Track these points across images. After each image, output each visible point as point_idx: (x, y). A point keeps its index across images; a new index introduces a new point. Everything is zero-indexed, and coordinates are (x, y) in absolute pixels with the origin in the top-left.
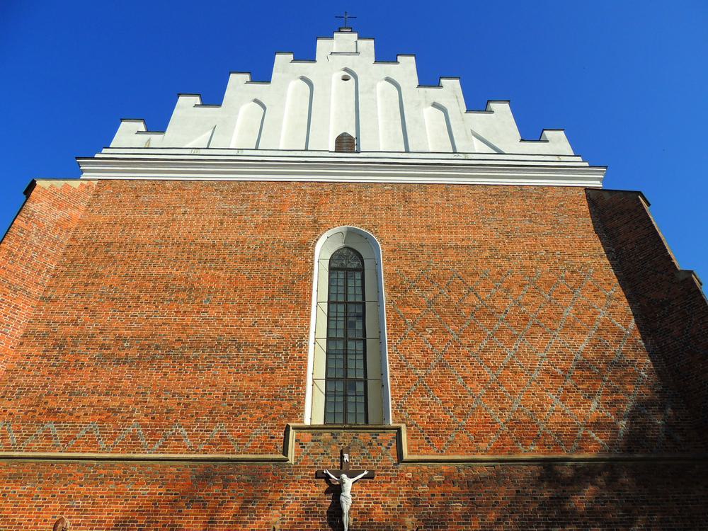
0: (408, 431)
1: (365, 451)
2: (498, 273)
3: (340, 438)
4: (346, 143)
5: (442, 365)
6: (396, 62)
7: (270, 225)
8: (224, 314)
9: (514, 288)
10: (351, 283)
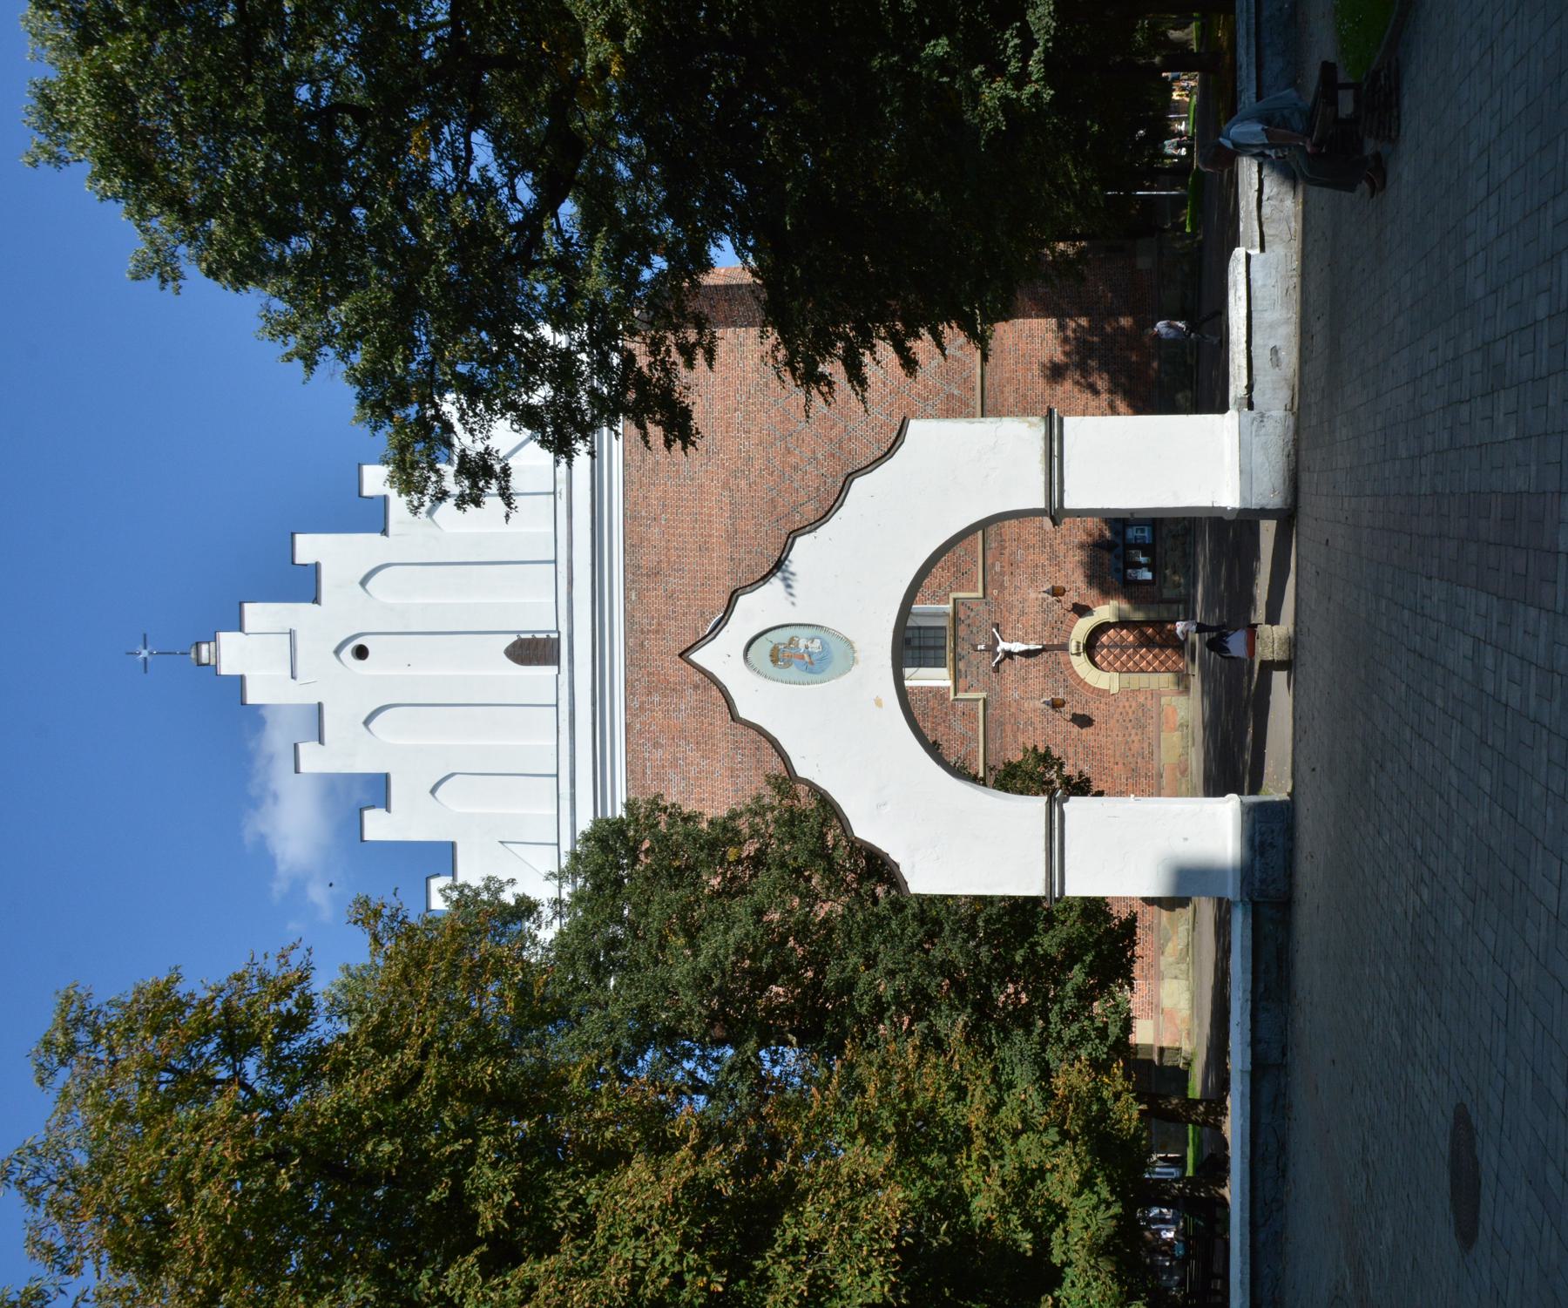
0: (957, 590)
2: (771, 474)
4: (532, 651)
6: (316, 567)
9: (792, 460)
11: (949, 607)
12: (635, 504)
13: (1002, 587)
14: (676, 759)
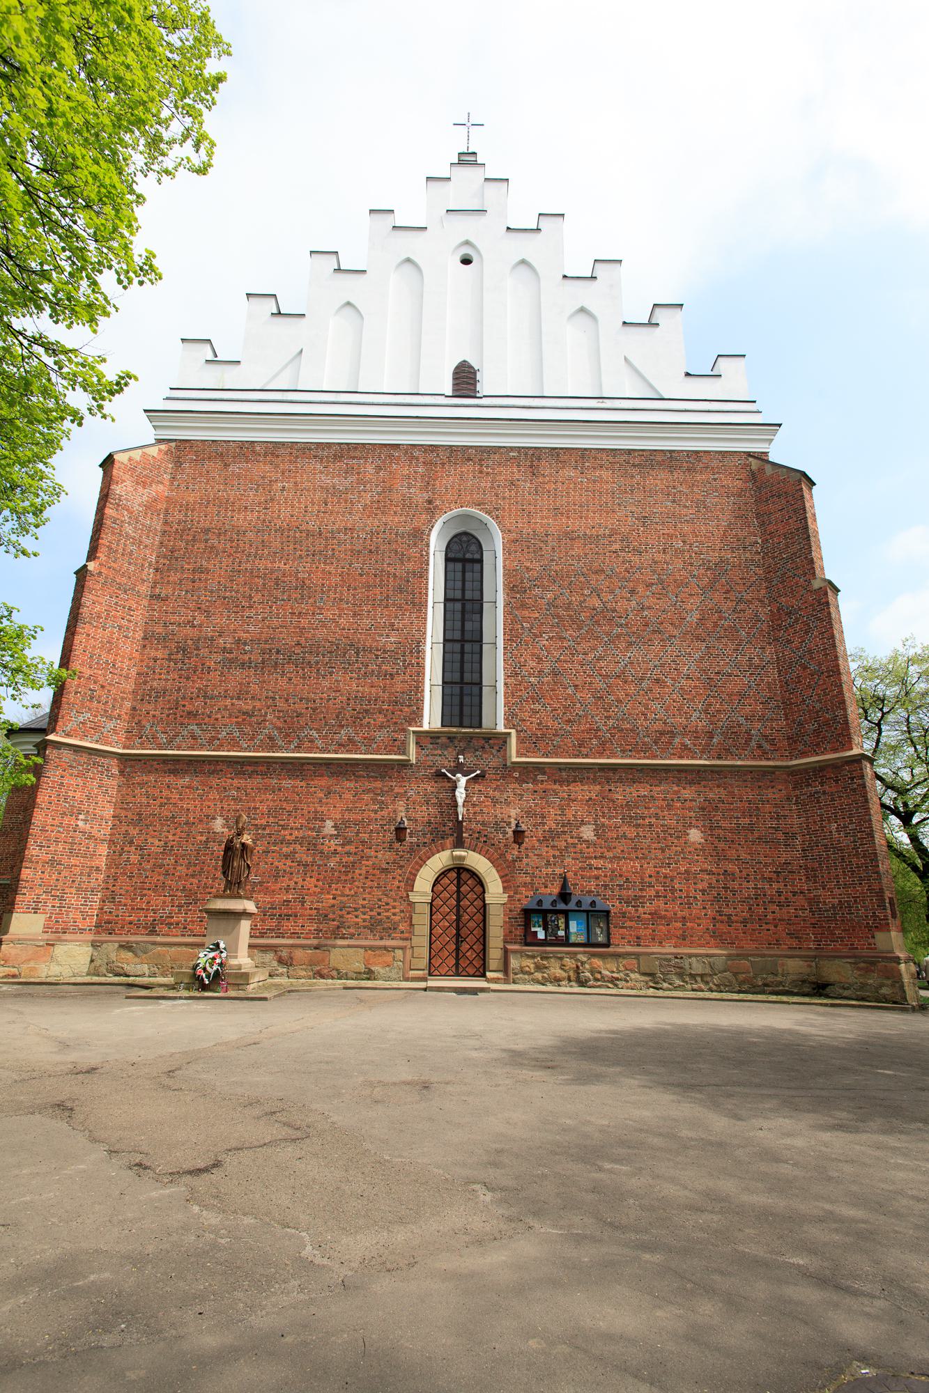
0: (518, 737)
3: (456, 742)
4: (465, 380)
5: (555, 673)
7: (379, 507)
8: (340, 616)
9: (640, 589)
10: (468, 575)
11: (501, 728)
12: (595, 458)
13: (521, 781)
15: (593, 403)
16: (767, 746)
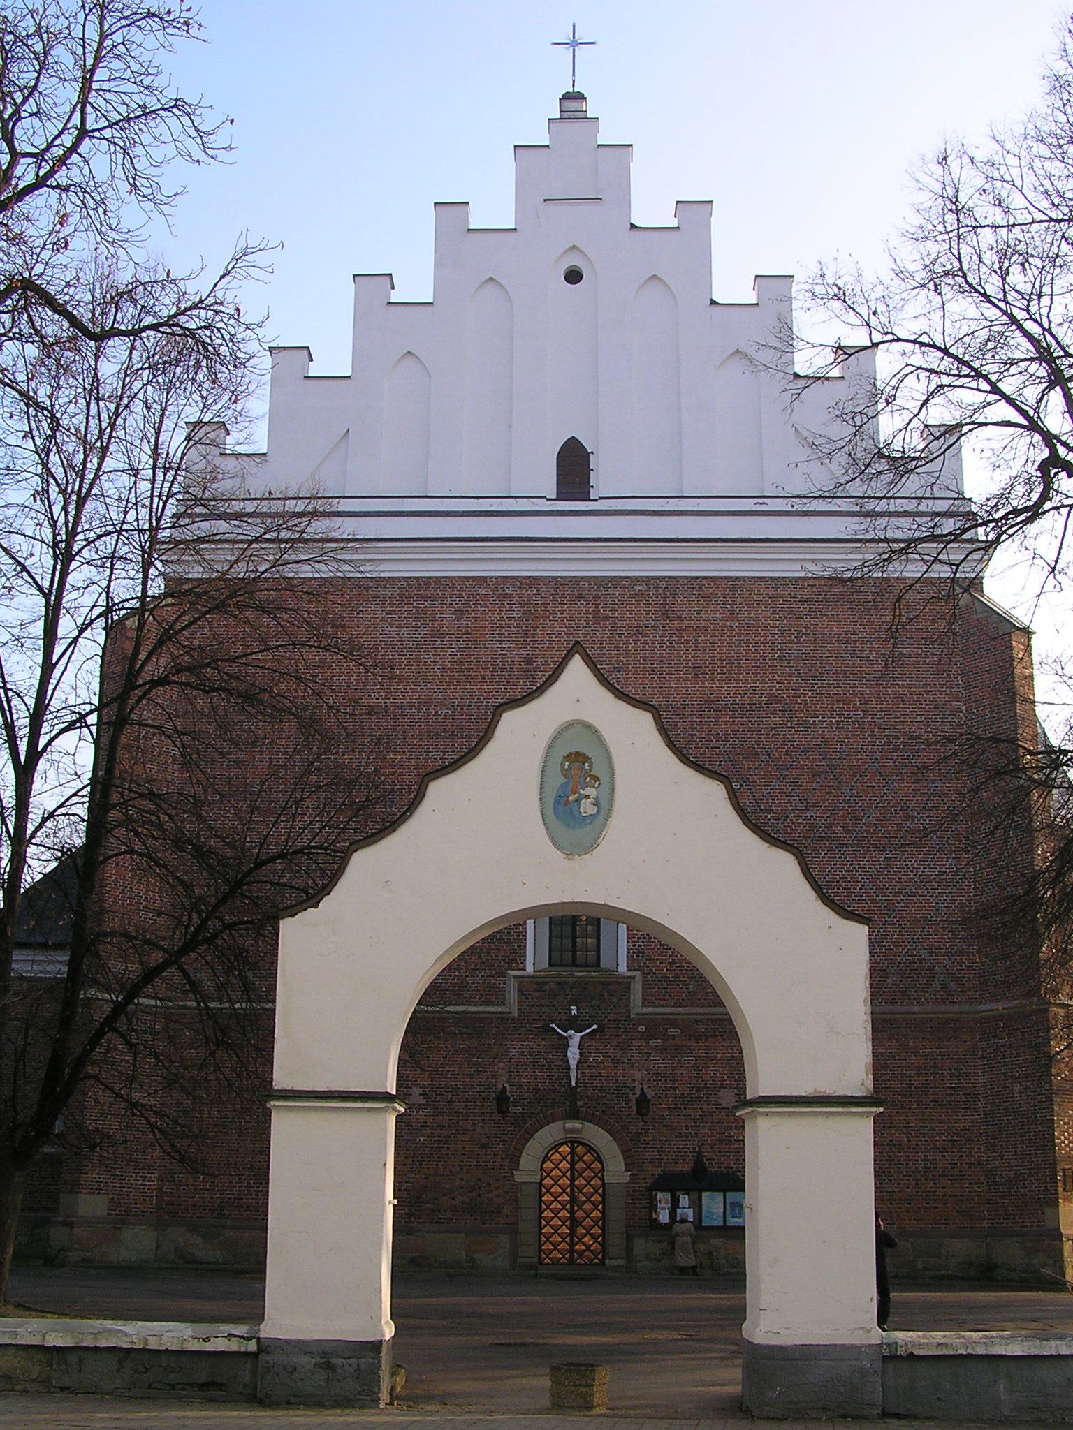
1: (594, 1002)
4: (574, 467)
9: (805, 779)
12: (750, 591)
13: (648, 1036)
14: (442, 636)
15: (749, 505)
16: (952, 986)
